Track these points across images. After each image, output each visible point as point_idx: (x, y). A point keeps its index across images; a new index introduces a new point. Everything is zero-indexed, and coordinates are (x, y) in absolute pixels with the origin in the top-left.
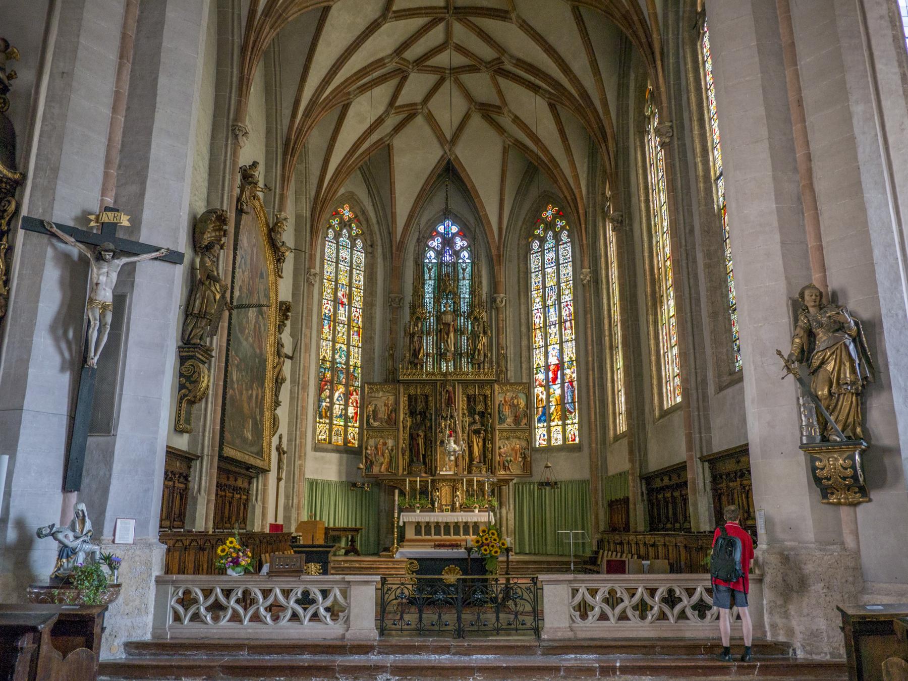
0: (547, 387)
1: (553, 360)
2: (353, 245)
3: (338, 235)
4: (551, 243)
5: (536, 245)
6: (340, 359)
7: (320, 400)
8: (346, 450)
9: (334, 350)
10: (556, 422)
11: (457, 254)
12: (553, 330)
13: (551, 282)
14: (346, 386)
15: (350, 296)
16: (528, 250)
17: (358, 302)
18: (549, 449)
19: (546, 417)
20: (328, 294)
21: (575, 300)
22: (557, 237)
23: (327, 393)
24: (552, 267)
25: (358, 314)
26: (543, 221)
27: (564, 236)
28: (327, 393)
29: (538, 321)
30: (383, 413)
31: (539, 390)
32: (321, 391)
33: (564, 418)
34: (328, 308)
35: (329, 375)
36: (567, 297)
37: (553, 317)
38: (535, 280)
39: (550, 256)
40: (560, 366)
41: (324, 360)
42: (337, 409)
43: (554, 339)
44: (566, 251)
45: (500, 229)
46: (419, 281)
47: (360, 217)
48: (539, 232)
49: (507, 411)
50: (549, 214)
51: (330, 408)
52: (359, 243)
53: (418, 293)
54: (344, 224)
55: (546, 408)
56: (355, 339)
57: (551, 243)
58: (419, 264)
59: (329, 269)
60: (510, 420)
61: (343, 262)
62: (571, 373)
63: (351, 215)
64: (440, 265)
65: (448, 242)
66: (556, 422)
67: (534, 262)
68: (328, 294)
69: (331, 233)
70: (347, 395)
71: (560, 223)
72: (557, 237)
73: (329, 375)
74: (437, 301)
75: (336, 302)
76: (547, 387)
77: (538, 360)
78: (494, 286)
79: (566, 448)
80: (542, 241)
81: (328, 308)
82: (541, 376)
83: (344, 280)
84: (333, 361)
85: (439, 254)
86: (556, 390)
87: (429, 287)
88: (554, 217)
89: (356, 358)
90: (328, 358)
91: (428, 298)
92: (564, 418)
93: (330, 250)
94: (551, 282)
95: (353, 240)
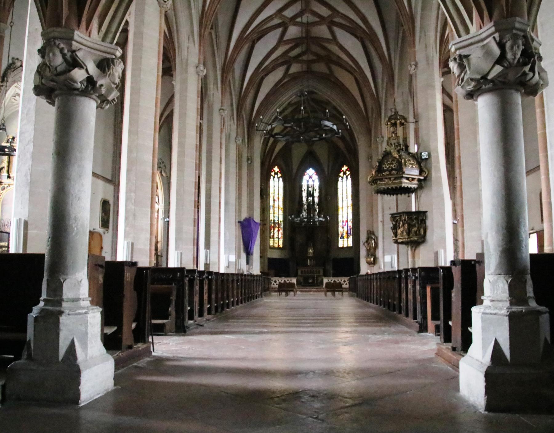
0: (343, 228)
1: (345, 220)
3: (274, 177)
5: (340, 179)
6: (276, 219)
7: (270, 233)
8: (279, 248)
10: (345, 239)
12: (345, 209)
14: (278, 228)
16: (337, 181)
18: (343, 248)
19: (342, 237)
21: (352, 200)
22: (347, 177)
23: (272, 230)
24: (345, 186)
26: (343, 171)
27: (349, 177)
28: (272, 230)
29: (340, 205)
31: (340, 229)
32: (270, 230)
33: (348, 238)
35: (273, 225)
37: (345, 205)
40: (347, 221)
42: (276, 236)
45: (328, 173)
46: (301, 191)
47: (281, 171)
48: (341, 174)
50: (345, 168)
51: (273, 235)
52: (281, 179)
53: (301, 197)
55: (342, 234)
61: (277, 186)
62: (350, 224)
63: (278, 170)
66: (345, 239)
69: (272, 177)
70: (278, 231)
71: (348, 173)
72: (347, 177)
73: (273, 225)
74: (307, 199)
75: (274, 200)
76: (343, 228)
77: (340, 218)
78: (326, 195)
79: (348, 247)
80: (342, 178)
82: (340, 224)
84: (274, 221)
85: (308, 181)
86: (345, 229)
87: (304, 194)
88: (346, 170)
89: (281, 219)
90: (273, 219)
91: (304, 199)
92: (348, 238)
95: (279, 178)
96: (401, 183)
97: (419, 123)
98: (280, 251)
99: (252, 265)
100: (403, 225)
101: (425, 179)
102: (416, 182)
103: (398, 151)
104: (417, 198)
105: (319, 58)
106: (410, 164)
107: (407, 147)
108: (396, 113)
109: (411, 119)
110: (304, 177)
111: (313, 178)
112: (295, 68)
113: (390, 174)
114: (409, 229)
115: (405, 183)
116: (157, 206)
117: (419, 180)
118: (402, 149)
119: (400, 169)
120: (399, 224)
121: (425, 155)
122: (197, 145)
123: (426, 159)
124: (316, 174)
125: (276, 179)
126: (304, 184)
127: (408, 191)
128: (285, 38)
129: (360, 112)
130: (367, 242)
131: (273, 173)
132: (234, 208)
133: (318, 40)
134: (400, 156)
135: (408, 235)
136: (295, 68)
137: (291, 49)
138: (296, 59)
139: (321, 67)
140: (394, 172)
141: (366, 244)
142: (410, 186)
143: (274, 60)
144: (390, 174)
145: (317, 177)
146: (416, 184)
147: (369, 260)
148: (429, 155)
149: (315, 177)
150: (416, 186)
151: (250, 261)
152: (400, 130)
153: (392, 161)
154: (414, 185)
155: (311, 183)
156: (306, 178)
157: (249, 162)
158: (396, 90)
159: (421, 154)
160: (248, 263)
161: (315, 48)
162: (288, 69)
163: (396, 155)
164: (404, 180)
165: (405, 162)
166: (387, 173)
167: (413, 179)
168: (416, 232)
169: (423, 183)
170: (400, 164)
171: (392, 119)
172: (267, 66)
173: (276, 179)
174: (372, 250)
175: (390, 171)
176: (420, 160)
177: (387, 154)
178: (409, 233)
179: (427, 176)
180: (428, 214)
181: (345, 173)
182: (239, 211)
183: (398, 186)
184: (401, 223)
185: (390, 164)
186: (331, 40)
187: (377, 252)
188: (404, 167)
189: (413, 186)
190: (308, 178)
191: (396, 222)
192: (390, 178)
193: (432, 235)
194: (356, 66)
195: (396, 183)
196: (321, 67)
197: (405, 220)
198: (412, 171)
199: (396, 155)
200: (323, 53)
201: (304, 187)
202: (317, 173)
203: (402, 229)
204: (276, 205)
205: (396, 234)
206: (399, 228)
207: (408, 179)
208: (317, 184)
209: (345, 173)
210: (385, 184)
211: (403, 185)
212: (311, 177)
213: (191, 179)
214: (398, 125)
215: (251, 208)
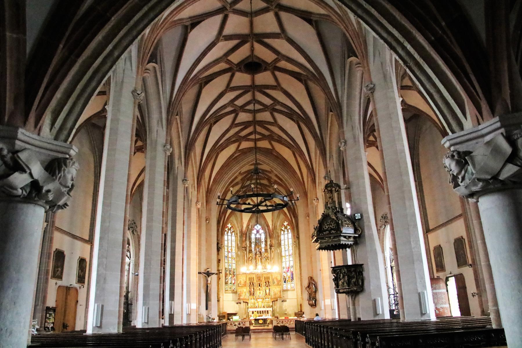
1: (288, 266)
2: (232, 234)
3: (228, 233)
4: (286, 232)
5: (282, 232)
9: (229, 266)
11: (260, 235)
13: (286, 243)
15: (232, 250)
17: (234, 251)
20: (226, 250)
22: (288, 231)
25: (234, 254)
27: (290, 230)
29: (283, 254)
30: (243, 282)
34: (226, 254)
36: (291, 248)
38: (282, 242)
39: (286, 236)
41: (226, 269)
42: (230, 282)
43: (288, 260)
44: (290, 235)
49: (275, 281)
54: (229, 229)
56: (233, 262)
57: (286, 232)
58: (250, 239)
59: (226, 243)
60: (276, 283)
64: (256, 238)
65: (258, 232)
67: (282, 237)
68: (226, 250)
71: (288, 227)
72: (288, 231)
75: (228, 252)
80: (284, 231)
81: (226, 254)
83: (230, 245)
85: (256, 235)
86: (289, 274)
88: (288, 225)
93: (226, 237)
94: (286, 243)
95: (231, 233)
96: (340, 240)
97: (351, 189)
98: (234, 294)
99: (211, 309)
100: (344, 277)
101: (360, 236)
102: (352, 239)
103: (335, 214)
104: (353, 252)
105: (264, 137)
106: (346, 224)
107: (342, 210)
108: (331, 182)
109: (343, 186)
110: (253, 232)
111: (260, 232)
112: (245, 145)
113: (330, 233)
114: (348, 280)
115: (343, 240)
116: (127, 260)
117: (354, 237)
118: (338, 212)
119: (338, 229)
120: (340, 276)
121: (358, 216)
122: (164, 181)
123: (359, 219)
124: (263, 229)
125: (229, 234)
126: (253, 236)
127: (344, 247)
128: (236, 122)
129: (298, 179)
130: (309, 286)
131: (227, 229)
132: (195, 262)
133: (262, 123)
134: (337, 218)
135: (349, 286)
136: (245, 145)
137: (242, 130)
138: (246, 138)
139: (264, 144)
140: (333, 231)
141: (308, 289)
142: (347, 243)
143: (227, 139)
144: (330, 233)
145: (263, 231)
146: (352, 241)
147: (311, 302)
148: (362, 216)
149: (261, 231)
150: (352, 243)
151: (209, 307)
152: (336, 195)
153: (331, 222)
154: (350, 242)
155: (258, 236)
156: (254, 232)
157: (208, 222)
158: (328, 162)
159: (354, 215)
160: (207, 309)
161: (259, 129)
162: (239, 146)
163: (334, 217)
164: (342, 238)
165: (342, 223)
166: (327, 232)
167: (350, 237)
168: (355, 283)
169: (358, 239)
170: (338, 224)
171: (329, 187)
172: (221, 144)
173: (229, 234)
174: (313, 294)
175: (330, 231)
176: (354, 220)
177: (325, 217)
178: (349, 284)
179: (361, 234)
180: (364, 266)
181: (286, 228)
182: (200, 263)
183: (337, 243)
184: (342, 275)
185: (329, 225)
186: (273, 123)
187: (317, 296)
188: (341, 227)
189: (349, 243)
190: (256, 233)
191: (337, 275)
192: (330, 237)
193: (370, 285)
194: (294, 143)
195: (335, 241)
196: (264, 144)
197: (345, 273)
198: (348, 230)
199: (334, 217)
200: (267, 133)
201: (253, 240)
202: (263, 228)
203: (342, 281)
204: (230, 255)
205: (337, 285)
206: (340, 280)
207: (345, 237)
208: (263, 237)
209: (286, 228)
210: (325, 242)
211: (342, 242)
212: (258, 232)
213: (158, 240)
214: (334, 192)
215: (209, 260)
